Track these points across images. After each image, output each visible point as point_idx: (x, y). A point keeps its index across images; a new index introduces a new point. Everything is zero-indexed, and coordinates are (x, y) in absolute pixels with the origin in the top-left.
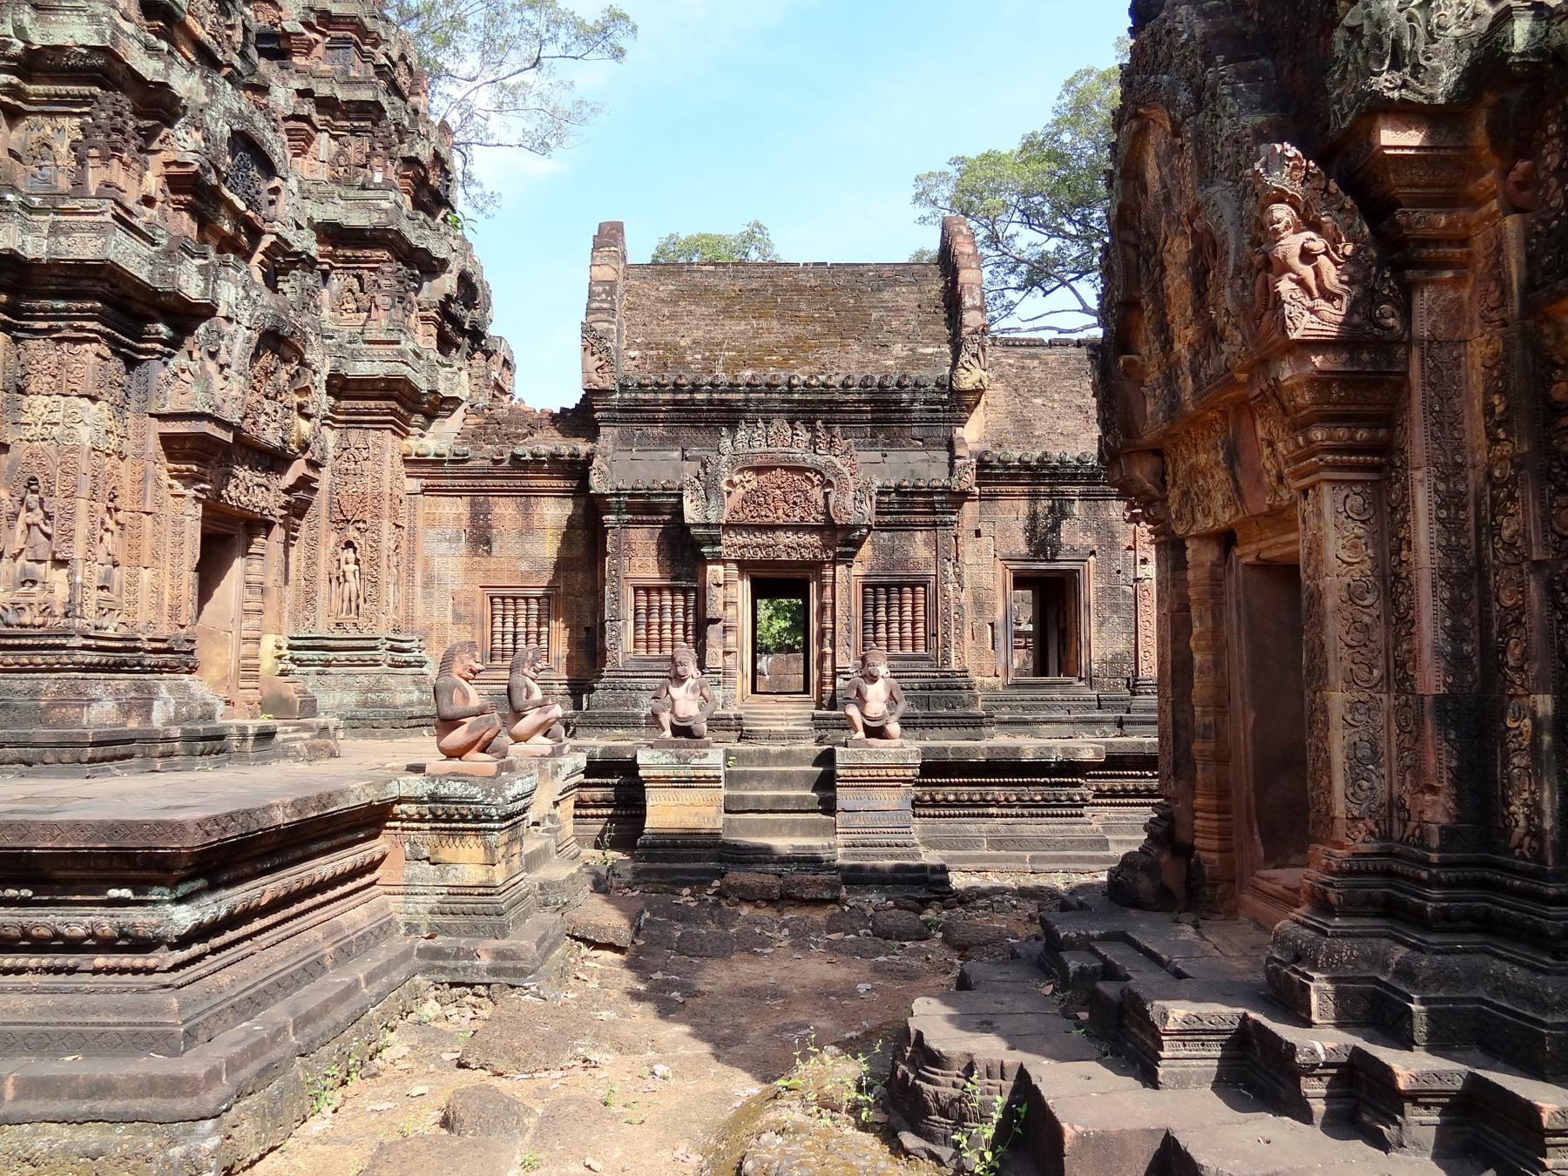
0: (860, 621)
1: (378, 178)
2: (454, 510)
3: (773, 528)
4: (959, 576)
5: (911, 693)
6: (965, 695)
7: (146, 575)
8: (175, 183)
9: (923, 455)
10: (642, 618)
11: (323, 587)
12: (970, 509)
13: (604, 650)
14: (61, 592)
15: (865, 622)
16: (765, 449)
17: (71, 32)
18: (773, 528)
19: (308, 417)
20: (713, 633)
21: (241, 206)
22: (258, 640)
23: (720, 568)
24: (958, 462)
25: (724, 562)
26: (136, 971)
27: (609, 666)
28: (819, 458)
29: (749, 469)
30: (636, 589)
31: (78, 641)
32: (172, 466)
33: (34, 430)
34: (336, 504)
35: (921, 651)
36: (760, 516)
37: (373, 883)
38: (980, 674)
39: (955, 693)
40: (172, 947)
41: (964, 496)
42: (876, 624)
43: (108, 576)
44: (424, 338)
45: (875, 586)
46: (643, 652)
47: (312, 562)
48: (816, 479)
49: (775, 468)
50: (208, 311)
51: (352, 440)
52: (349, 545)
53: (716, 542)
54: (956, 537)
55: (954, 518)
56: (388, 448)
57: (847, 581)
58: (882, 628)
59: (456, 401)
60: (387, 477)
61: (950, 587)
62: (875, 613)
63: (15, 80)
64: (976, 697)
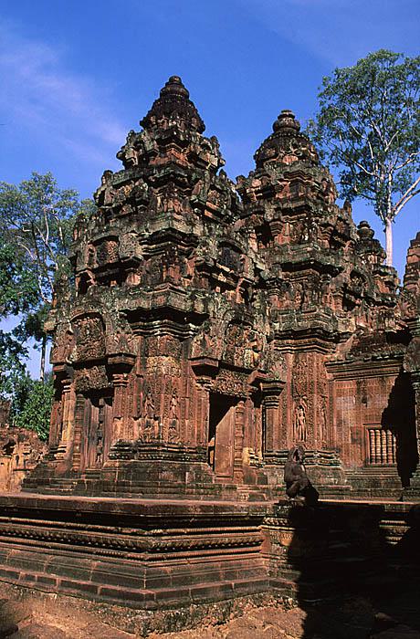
1: (307, 238)
2: (349, 386)
7: (187, 422)
8: (199, 268)
11: (289, 428)
14: (157, 429)
17: (161, 226)
19: (257, 352)
21: (227, 270)
22: (241, 450)
26: (138, 559)
31: (161, 449)
32: (197, 378)
33: (150, 369)
34: (293, 389)
37: (258, 551)
40: (149, 552)
43: (174, 423)
44: (336, 307)
47: (285, 415)
50: (206, 316)
51: (300, 358)
52: (301, 407)
56: (318, 359)
59: (351, 334)
60: (315, 374)
63: (146, 246)
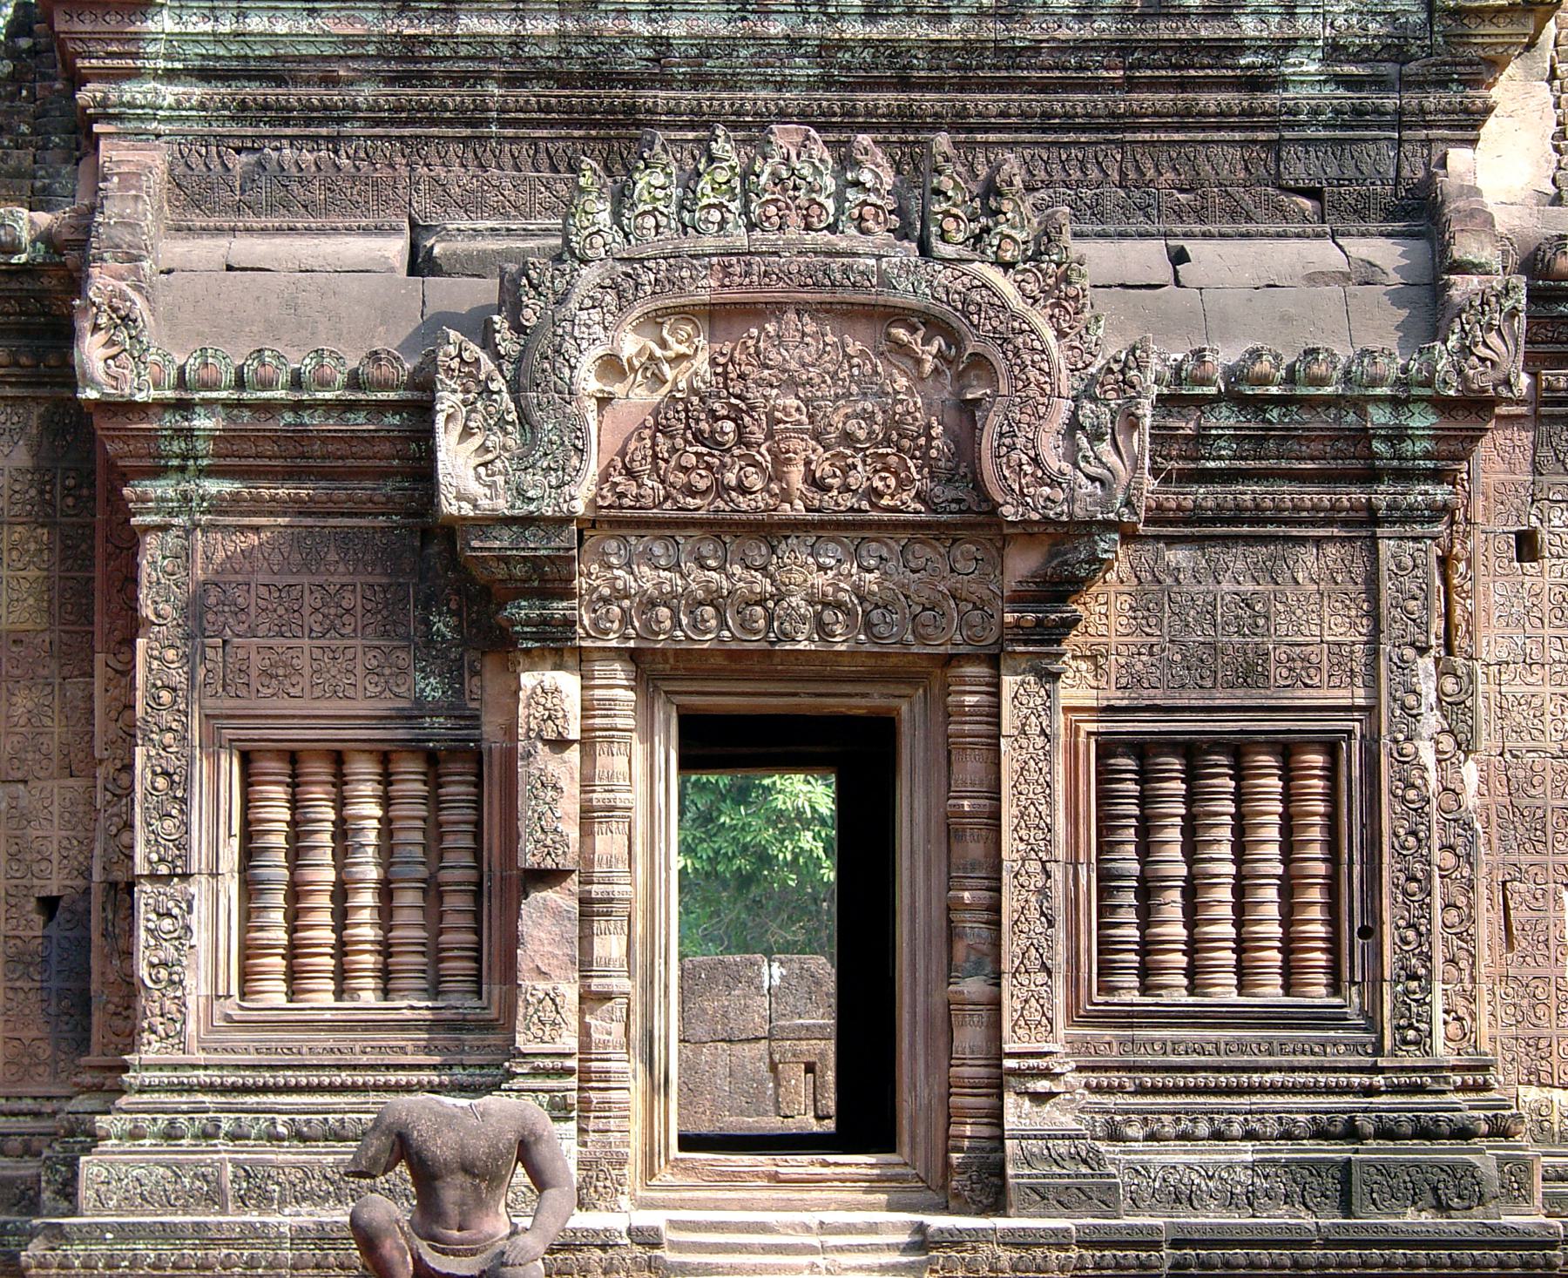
0: (1088, 878)
3: (770, 531)
4: (1455, 708)
5: (1285, 1151)
6: (1485, 1158)
9: (1325, 254)
10: (275, 868)
12: (1499, 459)
13: (129, 987)
15: (1107, 881)
16: (739, 237)
18: (770, 531)
20: (543, 922)
23: (568, 683)
24: (1463, 287)
25: (582, 660)
27: (151, 1050)
28: (944, 275)
29: (685, 313)
30: (246, 759)
35: (1317, 993)
36: (722, 489)
38: (1535, 1078)
39: (1444, 1152)
41: (1472, 410)
42: (1148, 890)
45: (1144, 750)
46: (274, 993)
48: (929, 351)
49: (776, 309)
53: (551, 580)
54: (1445, 562)
55: (1441, 493)
57: (1043, 731)
58: (1172, 905)
61: (1428, 756)
62: (1146, 848)
64: (1525, 1165)
